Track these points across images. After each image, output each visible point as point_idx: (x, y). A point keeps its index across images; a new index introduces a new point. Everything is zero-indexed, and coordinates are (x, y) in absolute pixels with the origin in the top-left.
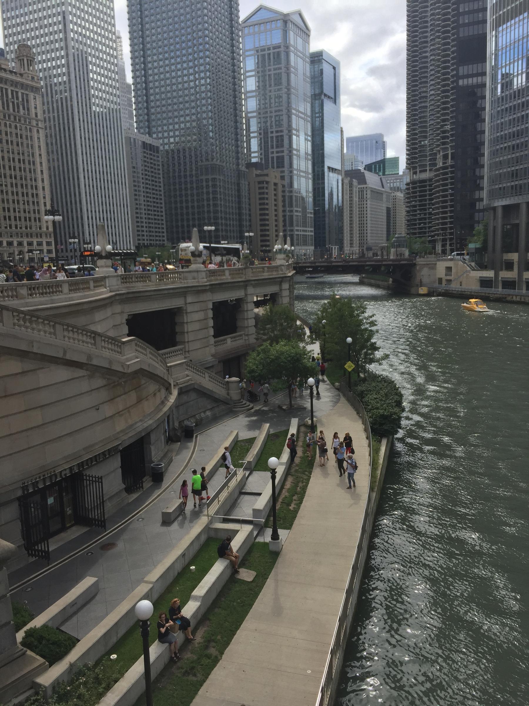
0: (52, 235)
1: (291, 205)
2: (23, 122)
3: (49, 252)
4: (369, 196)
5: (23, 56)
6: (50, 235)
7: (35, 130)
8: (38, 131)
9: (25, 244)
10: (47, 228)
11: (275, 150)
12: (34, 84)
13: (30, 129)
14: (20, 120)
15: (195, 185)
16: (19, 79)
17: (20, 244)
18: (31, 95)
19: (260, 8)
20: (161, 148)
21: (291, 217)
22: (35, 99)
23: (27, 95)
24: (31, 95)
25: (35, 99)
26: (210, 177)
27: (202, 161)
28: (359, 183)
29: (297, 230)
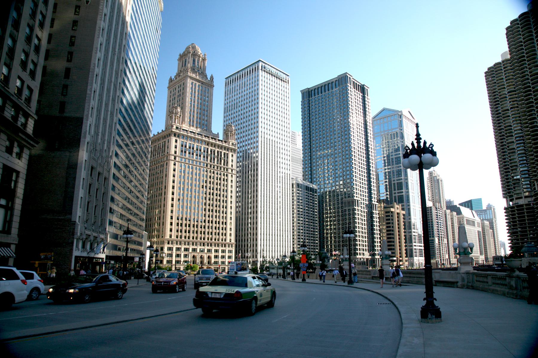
0: (234, 245)
1: (410, 228)
2: (222, 170)
3: (230, 257)
4: (465, 223)
5: (229, 131)
6: (232, 245)
7: (230, 175)
8: (232, 176)
11: (397, 191)
14: (220, 169)
15: (340, 214)
17: (209, 251)
18: (230, 154)
19: (384, 110)
20: (318, 191)
21: (411, 236)
22: (232, 156)
23: (227, 154)
25: (232, 156)
26: (351, 208)
27: (345, 197)
28: (457, 214)
29: (415, 246)
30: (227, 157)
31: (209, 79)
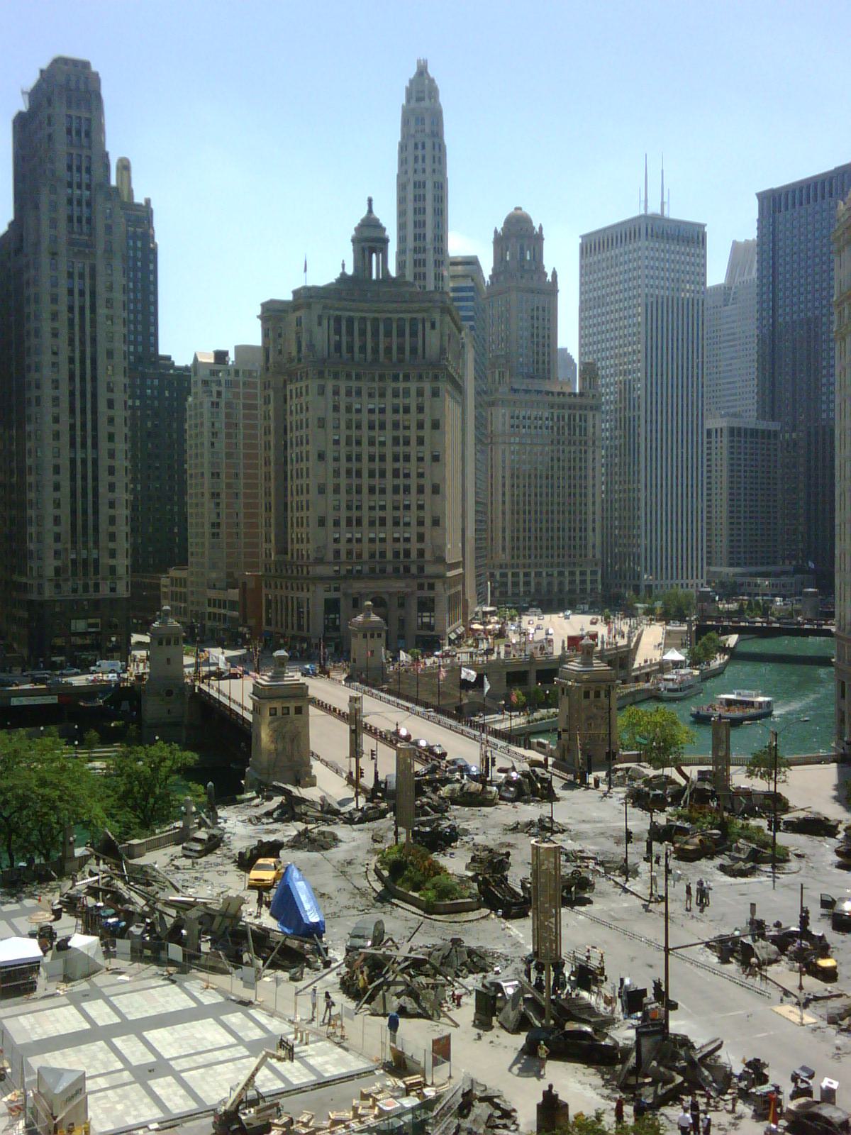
0: (600, 565)
9: (567, 574)
10: (594, 556)
12: (594, 402)
13: (585, 452)
16: (578, 400)
18: (590, 414)
22: (594, 416)
23: (586, 416)
24: (590, 414)
25: (594, 416)
30: (585, 421)
31: (549, 278)
